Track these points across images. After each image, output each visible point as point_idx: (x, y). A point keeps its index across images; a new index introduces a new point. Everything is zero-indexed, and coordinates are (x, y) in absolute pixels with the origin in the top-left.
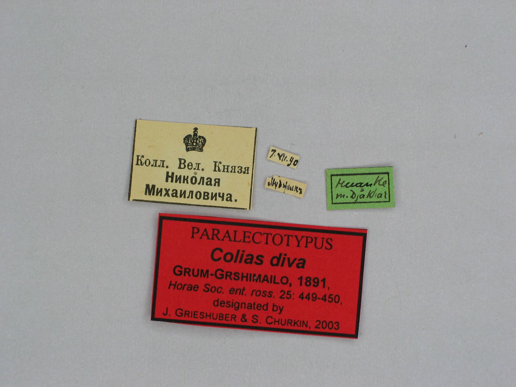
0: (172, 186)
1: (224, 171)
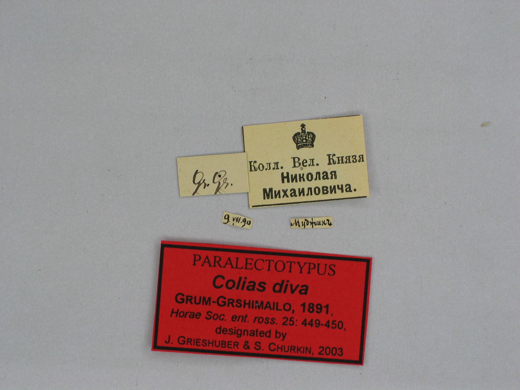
0: (289, 186)
1: (339, 163)
